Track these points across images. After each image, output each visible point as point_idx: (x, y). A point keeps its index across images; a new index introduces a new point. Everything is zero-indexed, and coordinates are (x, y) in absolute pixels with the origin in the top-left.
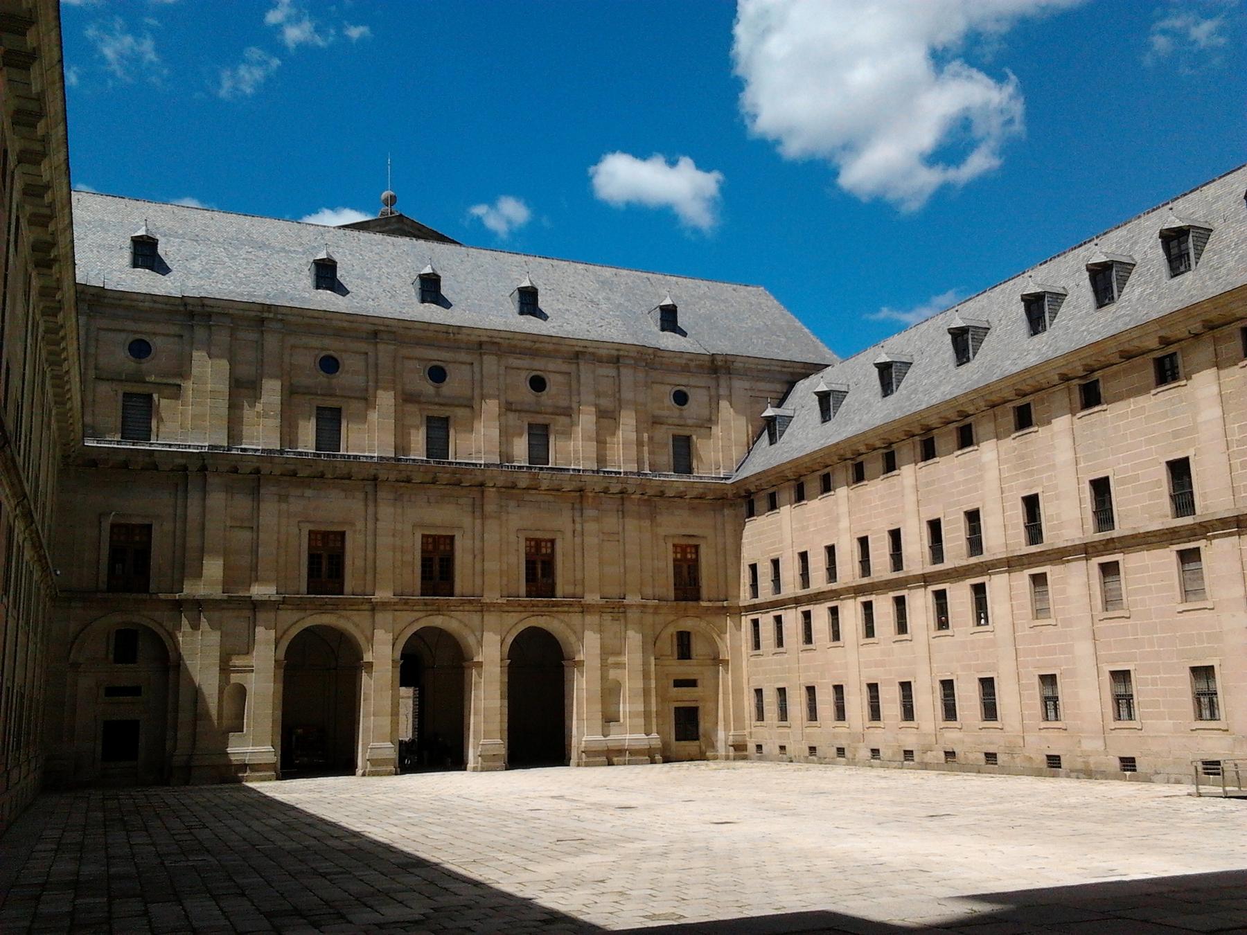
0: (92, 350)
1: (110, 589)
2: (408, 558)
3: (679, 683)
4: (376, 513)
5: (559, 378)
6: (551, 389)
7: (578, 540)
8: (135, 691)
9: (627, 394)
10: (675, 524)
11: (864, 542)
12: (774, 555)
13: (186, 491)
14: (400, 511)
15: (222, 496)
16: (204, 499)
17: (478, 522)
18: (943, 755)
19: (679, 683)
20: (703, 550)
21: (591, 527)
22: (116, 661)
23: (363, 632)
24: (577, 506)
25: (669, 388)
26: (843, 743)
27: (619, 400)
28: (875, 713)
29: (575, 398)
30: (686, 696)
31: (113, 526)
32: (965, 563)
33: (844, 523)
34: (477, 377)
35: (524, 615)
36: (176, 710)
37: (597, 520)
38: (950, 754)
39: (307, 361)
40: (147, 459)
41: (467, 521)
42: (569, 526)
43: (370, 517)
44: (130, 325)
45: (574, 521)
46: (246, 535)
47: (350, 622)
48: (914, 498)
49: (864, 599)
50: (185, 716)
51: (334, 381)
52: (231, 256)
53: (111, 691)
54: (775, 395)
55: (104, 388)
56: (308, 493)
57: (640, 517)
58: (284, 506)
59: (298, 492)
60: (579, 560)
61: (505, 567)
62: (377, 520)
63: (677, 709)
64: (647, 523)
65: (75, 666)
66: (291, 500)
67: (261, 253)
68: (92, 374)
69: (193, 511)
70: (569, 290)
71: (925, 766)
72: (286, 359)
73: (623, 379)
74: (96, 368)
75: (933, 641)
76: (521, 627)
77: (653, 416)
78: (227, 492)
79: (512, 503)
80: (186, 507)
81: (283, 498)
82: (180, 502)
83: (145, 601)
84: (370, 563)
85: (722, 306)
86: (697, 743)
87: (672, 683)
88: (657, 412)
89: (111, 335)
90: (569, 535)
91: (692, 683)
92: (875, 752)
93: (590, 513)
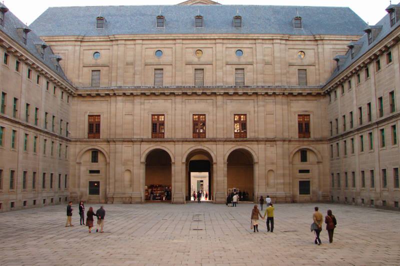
0: (81, 57)
1: (89, 138)
2: (188, 124)
3: (301, 171)
4: (175, 107)
5: (248, 50)
6: (245, 55)
7: (256, 115)
8: (98, 172)
9: (277, 54)
10: (300, 106)
11: (360, 108)
12: (336, 118)
13: (110, 103)
14: (184, 106)
15: (122, 104)
16: (116, 106)
17: (215, 109)
18: (382, 202)
19: (301, 171)
20: (311, 116)
21: (261, 109)
22: (92, 162)
23: (171, 152)
24: (256, 101)
25: (296, 51)
26: (354, 196)
27: (274, 57)
28: (364, 185)
29: (255, 58)
30: (304, 177)
31: (89, 116)
32: (388, 116)
33: (355, 102)
34: (214, 52)
35: (234, 146)
36: (109, 179)
37: (264, 106)
38: (384, 202)
39: (151, 52)
40: (97, 93)
41: (211, 108)
42: (252, 109)
43: (174, 109)
44: (93, 48)
45: (254, 107)
46: (129, 118)
47: (168, 148)
48: (374, 88)
49: (360, 135)
50: (112, 181)
51: (161, 59)
52: (131, 19)
53: (91, 172)
54: (344, 50)
55: (86, 69)
56: (151, 101)
57: (282, 104)
58: (142, 106)
59: (148, 101)
60: (256, 123)
61: (225, 126)
62: (175, 110)
63: (300, 181)
64: (285, 107)
65: (79, 163)
66: (146, 104)
67: (142, 18)
68: (81, 66)
69: (113, 110)
70: (259, 16)
71: (377, 207)
72: (143, 53)
73: (275, 48)
74: (83, 63)
75: (381, 152)
76: (232, 150)
77: (290, 63)
78: (123, 102)
79: (228, 101)
80: (110, 108)
81: (141, 104)
82: (109, 106)
83: (98, 141)
84: (173, 126)
85: (327, 16)
86: (309, 195)
87: (298, 171)
88: (291, 61)
89: (87, 51)
90: (252, 112)
91: (308, 171)
92: (363, 200)
93: (261, 103)
